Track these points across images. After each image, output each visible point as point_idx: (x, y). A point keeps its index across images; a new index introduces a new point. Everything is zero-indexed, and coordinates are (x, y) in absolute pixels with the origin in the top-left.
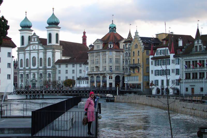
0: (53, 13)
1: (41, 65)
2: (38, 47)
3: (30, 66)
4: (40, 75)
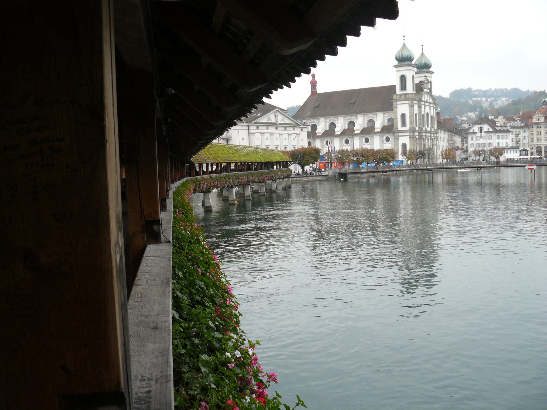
0: (422, 51)
1: (432, 127)
2: (430, 98)
3: (425, 127)
4: (431, 140)
